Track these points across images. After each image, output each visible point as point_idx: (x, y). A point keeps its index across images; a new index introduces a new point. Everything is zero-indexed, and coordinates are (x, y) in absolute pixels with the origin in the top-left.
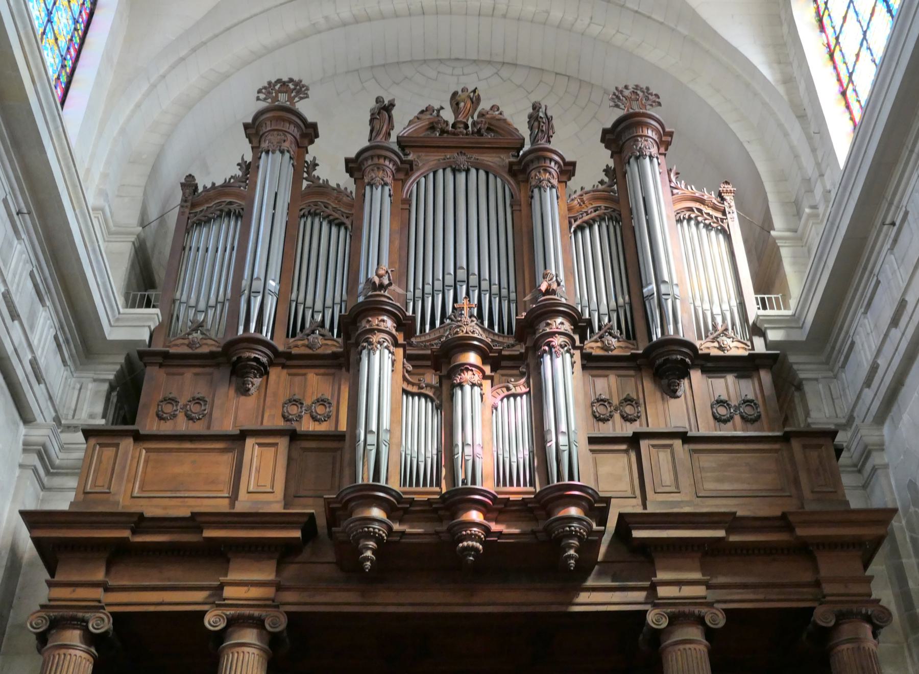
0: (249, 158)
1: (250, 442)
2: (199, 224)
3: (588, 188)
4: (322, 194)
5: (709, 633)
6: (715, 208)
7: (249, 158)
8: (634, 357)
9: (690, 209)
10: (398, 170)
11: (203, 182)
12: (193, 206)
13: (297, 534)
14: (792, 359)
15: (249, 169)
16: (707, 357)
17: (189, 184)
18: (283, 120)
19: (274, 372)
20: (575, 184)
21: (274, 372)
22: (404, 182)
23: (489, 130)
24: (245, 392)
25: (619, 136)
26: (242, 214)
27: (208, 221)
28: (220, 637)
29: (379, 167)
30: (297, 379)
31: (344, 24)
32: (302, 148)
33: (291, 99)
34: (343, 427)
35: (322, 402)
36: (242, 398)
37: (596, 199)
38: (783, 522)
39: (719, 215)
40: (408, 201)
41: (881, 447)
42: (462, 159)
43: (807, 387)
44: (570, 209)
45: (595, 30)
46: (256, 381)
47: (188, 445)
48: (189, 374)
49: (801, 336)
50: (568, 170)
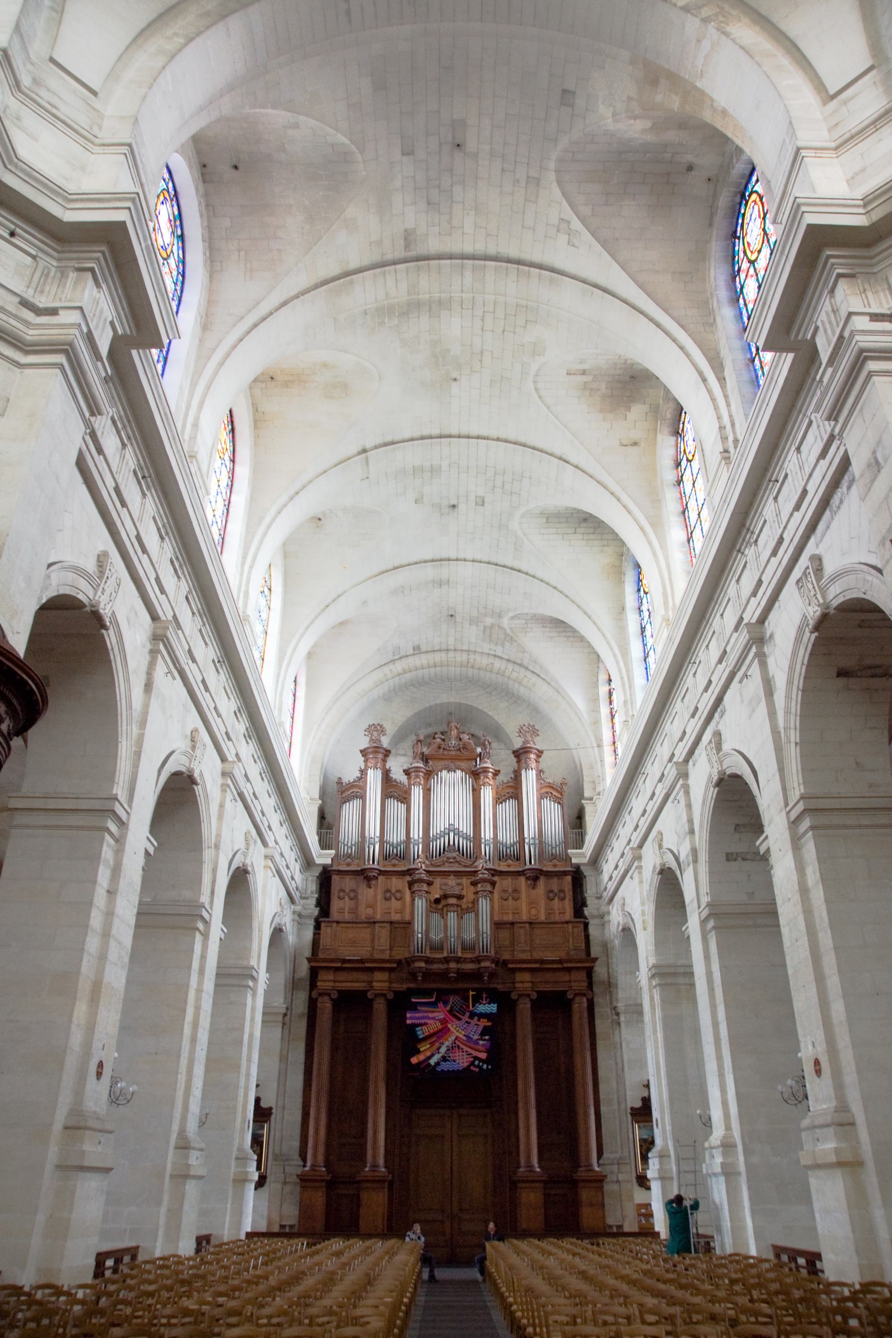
0: (363, 767)
1: (377, 925)
2: (345, 802)
3: (505, 781)
4: (394, 786)
5: (531, 1000)
6: (558, 792)
7: (363, 767)
8: (518, 872)
9: (547, 793)
10: (425, 774)
11: (345, 780)
12: (342, 793)
13: (395, 965)
14: (582, 868)
15: (363, 772)
16: (548, 872)
17: (339, 782)
18: (376, 752)
19: (381, 878)
20: (500, 778)
21: (381, 878)
22: (428, 779)
23: (464, 748)
24: (370, 887)
25: (521, 754)
26: (363, 797)
27: (349, 801)
28: (372, 1000)
29: (417, 777)
30: (388, 881)
31: (399, 675)
32: (384, 761)
33: (379, 735)
34: (407, 918)
35: (398, 891)
36: (369, 890)
37: (510, 787)
38: (560, 961)
39: (559, 796)
40: (429, 790)
41: (609, 913)
42: (452, 765)
43: (587, 878)
44: (497, 793)
45: (514, 675)
46: (374, 882)
47: (355, 925)
48: (348, 878)
49: (585, 860)
50: (496, 773)
